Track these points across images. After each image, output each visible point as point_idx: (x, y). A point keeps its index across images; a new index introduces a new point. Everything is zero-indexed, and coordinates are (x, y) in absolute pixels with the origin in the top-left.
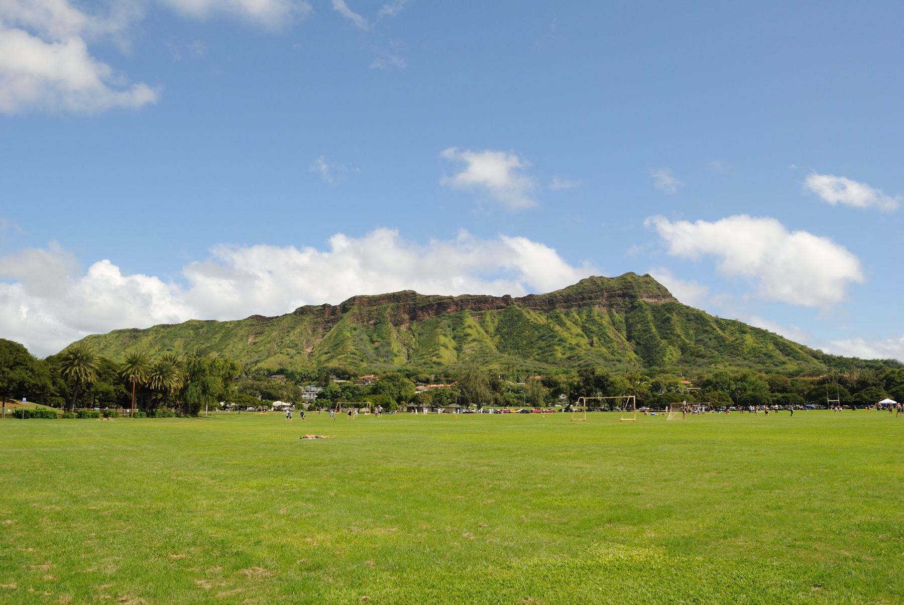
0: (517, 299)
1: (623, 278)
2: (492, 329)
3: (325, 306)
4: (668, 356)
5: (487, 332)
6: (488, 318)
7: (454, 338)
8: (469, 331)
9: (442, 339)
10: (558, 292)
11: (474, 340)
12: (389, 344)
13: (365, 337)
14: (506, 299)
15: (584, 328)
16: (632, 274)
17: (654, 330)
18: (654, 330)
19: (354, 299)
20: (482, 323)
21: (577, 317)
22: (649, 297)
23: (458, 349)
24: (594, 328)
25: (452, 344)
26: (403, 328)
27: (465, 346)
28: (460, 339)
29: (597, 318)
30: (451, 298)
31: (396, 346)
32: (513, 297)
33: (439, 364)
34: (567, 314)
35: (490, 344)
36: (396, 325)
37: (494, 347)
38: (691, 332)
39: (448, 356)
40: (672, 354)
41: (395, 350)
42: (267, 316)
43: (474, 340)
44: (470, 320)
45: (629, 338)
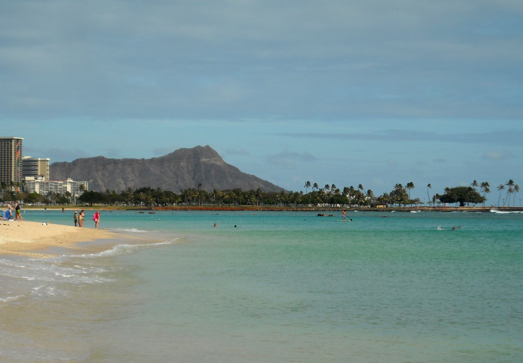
0: (147, 160)
3: (65, 163)
7: (122, 178)
8: (129, 176)
10: (165, 156)
11: (131, 180)
14: (143, 159)
16: (199, 147)
17: (203, 176)
22: (205, 158)
25: (123, 182)
26: (100, 173)
28: (125, 180)
30: (119, 160)
31: (100, 183)
32: (145, 159)
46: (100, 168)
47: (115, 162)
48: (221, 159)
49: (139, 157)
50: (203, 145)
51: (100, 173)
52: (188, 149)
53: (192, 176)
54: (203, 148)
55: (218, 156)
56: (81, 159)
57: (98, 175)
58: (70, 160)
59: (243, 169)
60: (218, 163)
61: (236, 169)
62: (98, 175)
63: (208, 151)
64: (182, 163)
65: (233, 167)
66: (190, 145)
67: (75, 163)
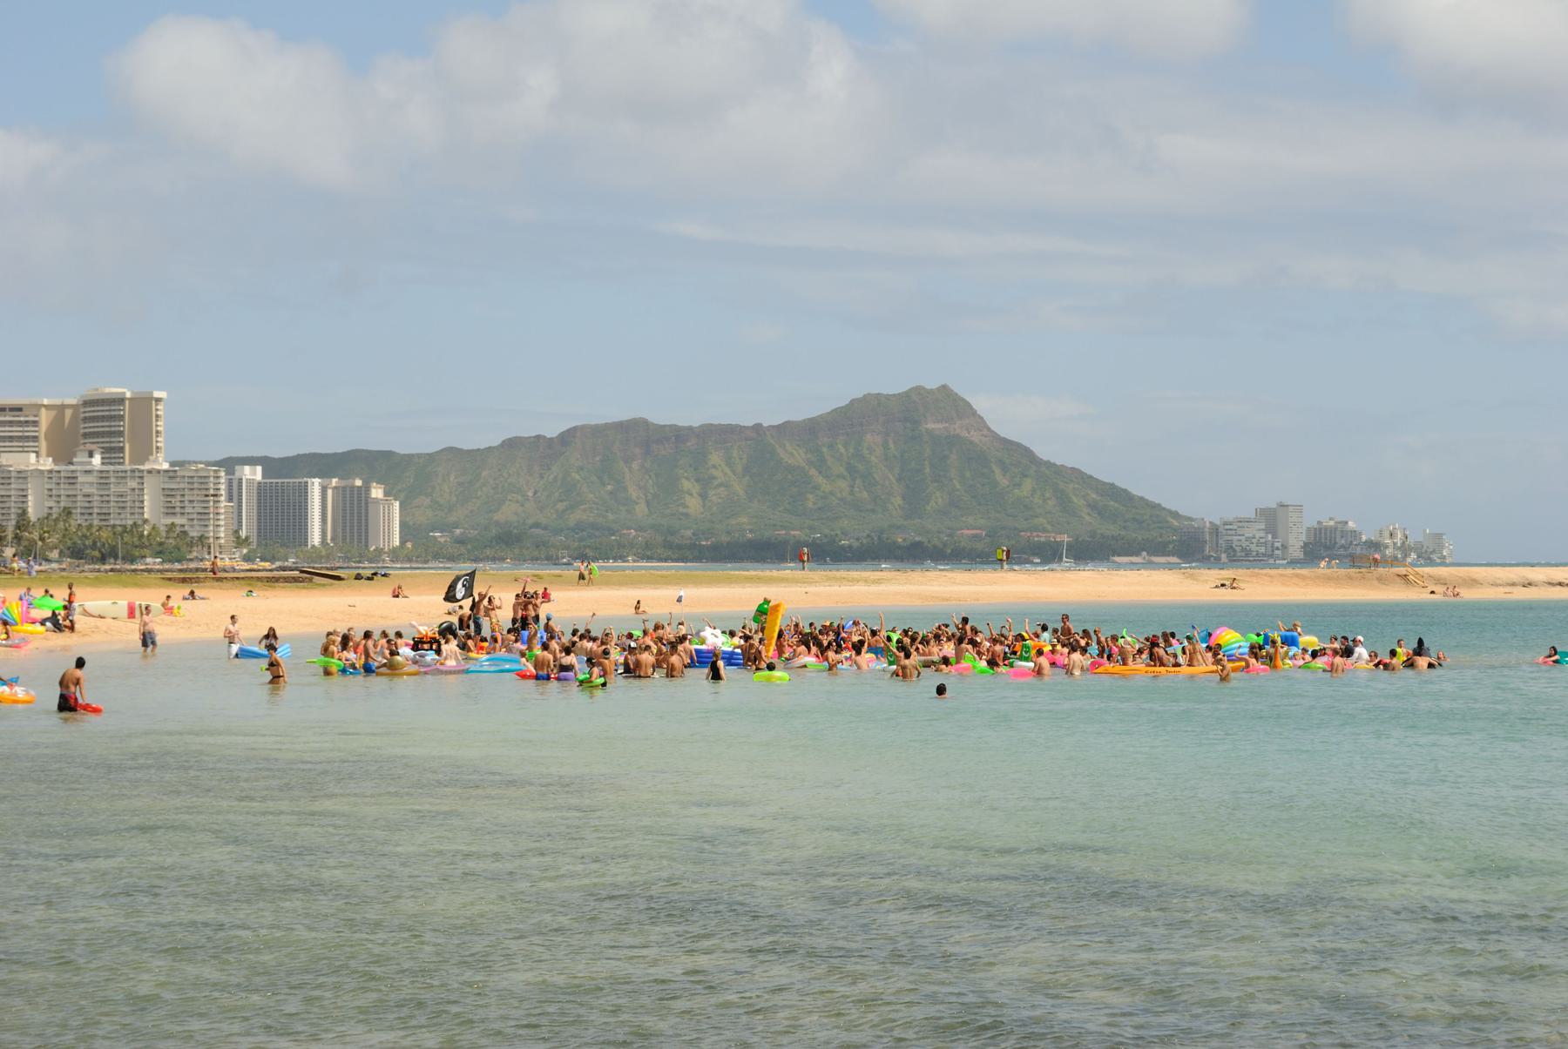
1: (907, 394)
2: (739, 468)
3: (538, 437)
4: (932, 503)
5: (734, 472)
6: (735, 453)
7: (697, 480)
9: (686, 485)
11: (721, 485)
12: (625, 489)
13: (594, 478)
14: (758, 427)
15: (851, 469)
17: (927, 470)
18: (927, 470)
19: (575, 429)
20: (729, 461)
21: (842, 450)
23: (703, 496)
24: (860, 467)
25: (696, 488)
26: (635, 466)
27: (711, 493)
28: (705, 483)
29: (866, 452)
30: (690, 428)
31: (633, 492)
33: (687, 515)
34: (831, 446)
35: (739, 489)
36: (626, 462)
37: (741, 492)
38: (968, 474)
39: (693, 504)
40: (938, 499)
41: (634, 495)
42: (466, 447)
43: (721, 485)
44: (715, 458)
45: (899, 480)
46: (637, 451)
47: (677, 435)
48: (981, 424)
49: (748, 422)
50: (932, 384)
51: (635, 466)
52: (888, 397)
53: (897, 471)
54: (930, 392)
55: (974, 413)
56: (583, 427)
57: (630, 469)
58: (552, 430)
59: (1043, 452)
60: (975, 437)
61: (1027, 452)
62: (630, 469)
63: (948, 402)
64: (868, 437)
65: (1019, 445)
66: (893, 383)
67: (567, 437)
